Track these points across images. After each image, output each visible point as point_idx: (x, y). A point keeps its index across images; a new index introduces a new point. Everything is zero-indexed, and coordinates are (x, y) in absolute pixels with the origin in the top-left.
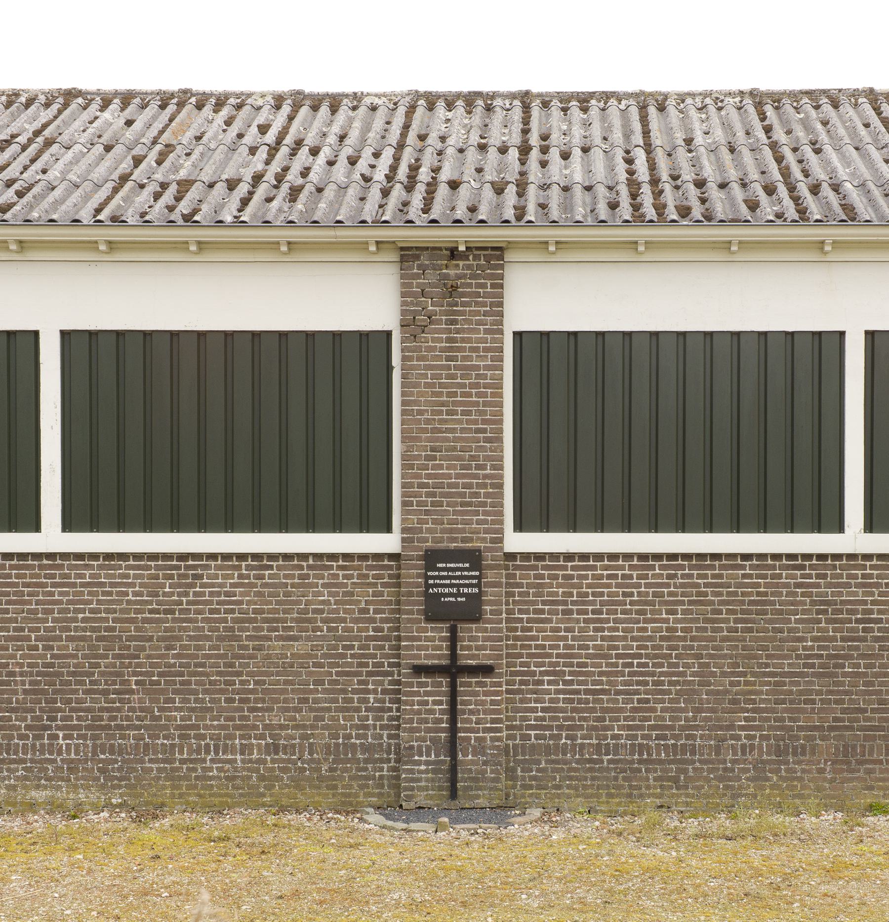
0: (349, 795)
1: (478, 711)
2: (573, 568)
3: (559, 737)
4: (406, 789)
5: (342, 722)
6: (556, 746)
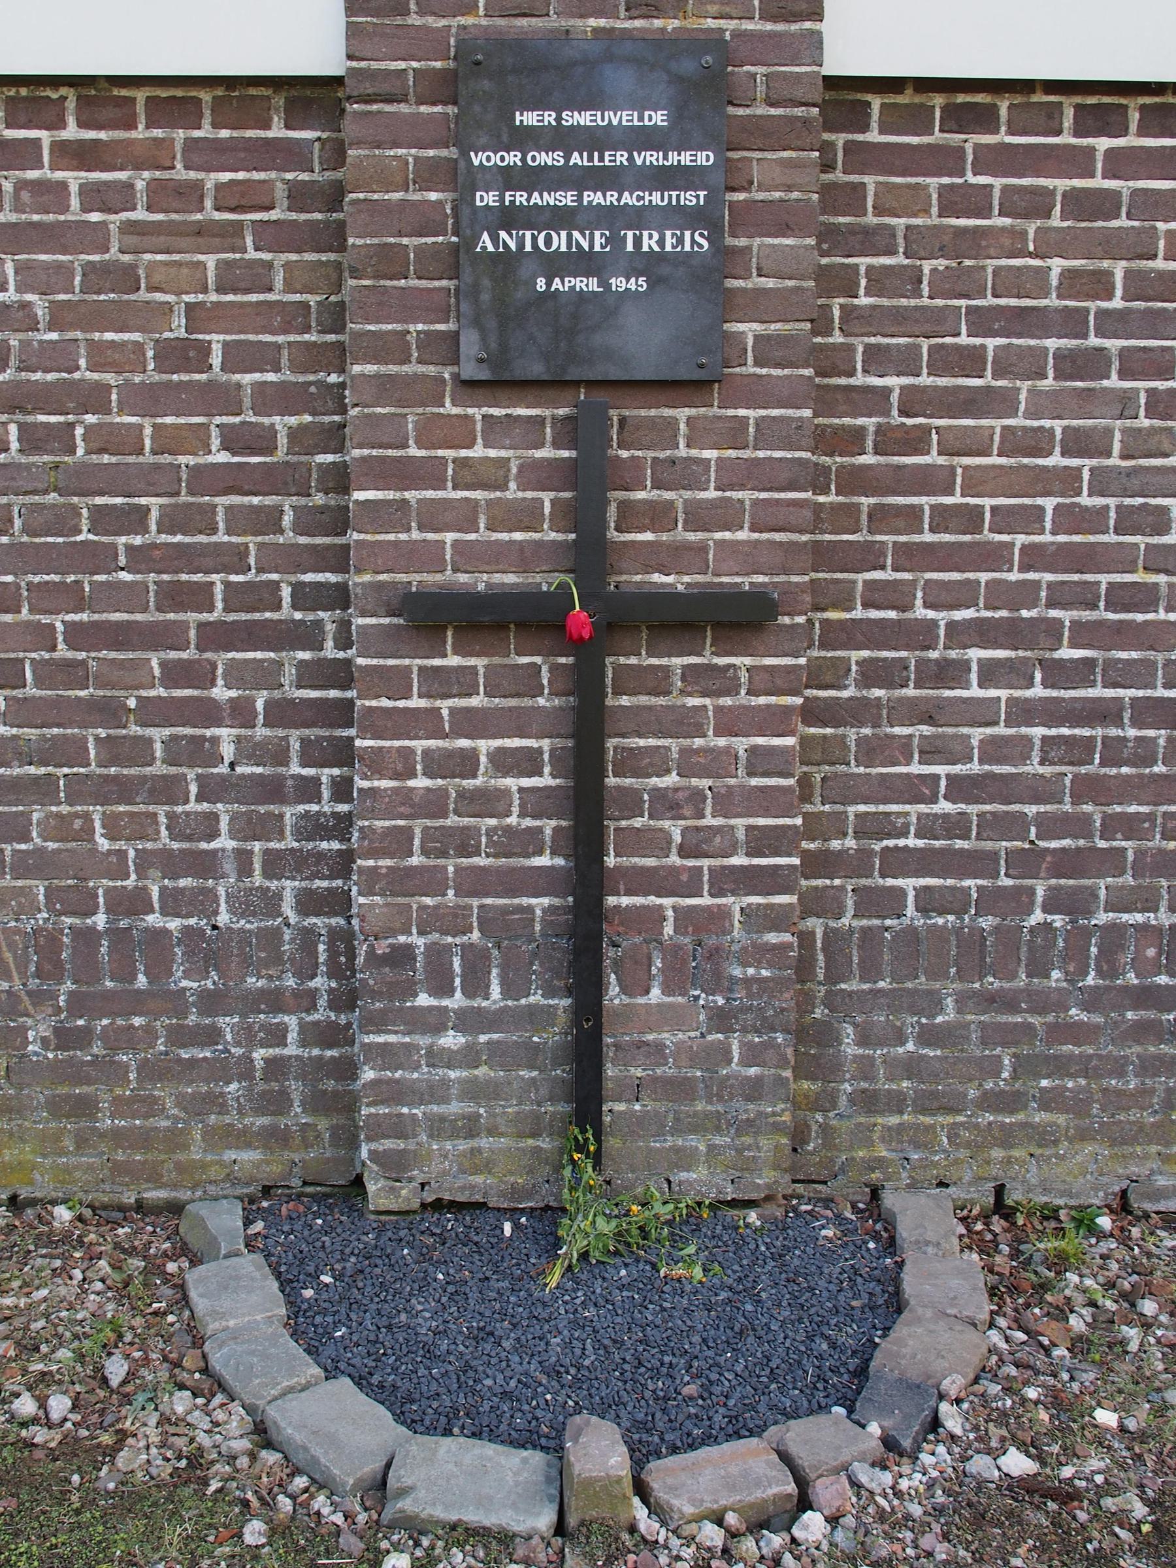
0: (144, 1140)
1: (697, 797)
2: (1118, 164)
3: (1021, 900)
4: (378, 1130)
5: (103, 844)
6: (1008, 937)
